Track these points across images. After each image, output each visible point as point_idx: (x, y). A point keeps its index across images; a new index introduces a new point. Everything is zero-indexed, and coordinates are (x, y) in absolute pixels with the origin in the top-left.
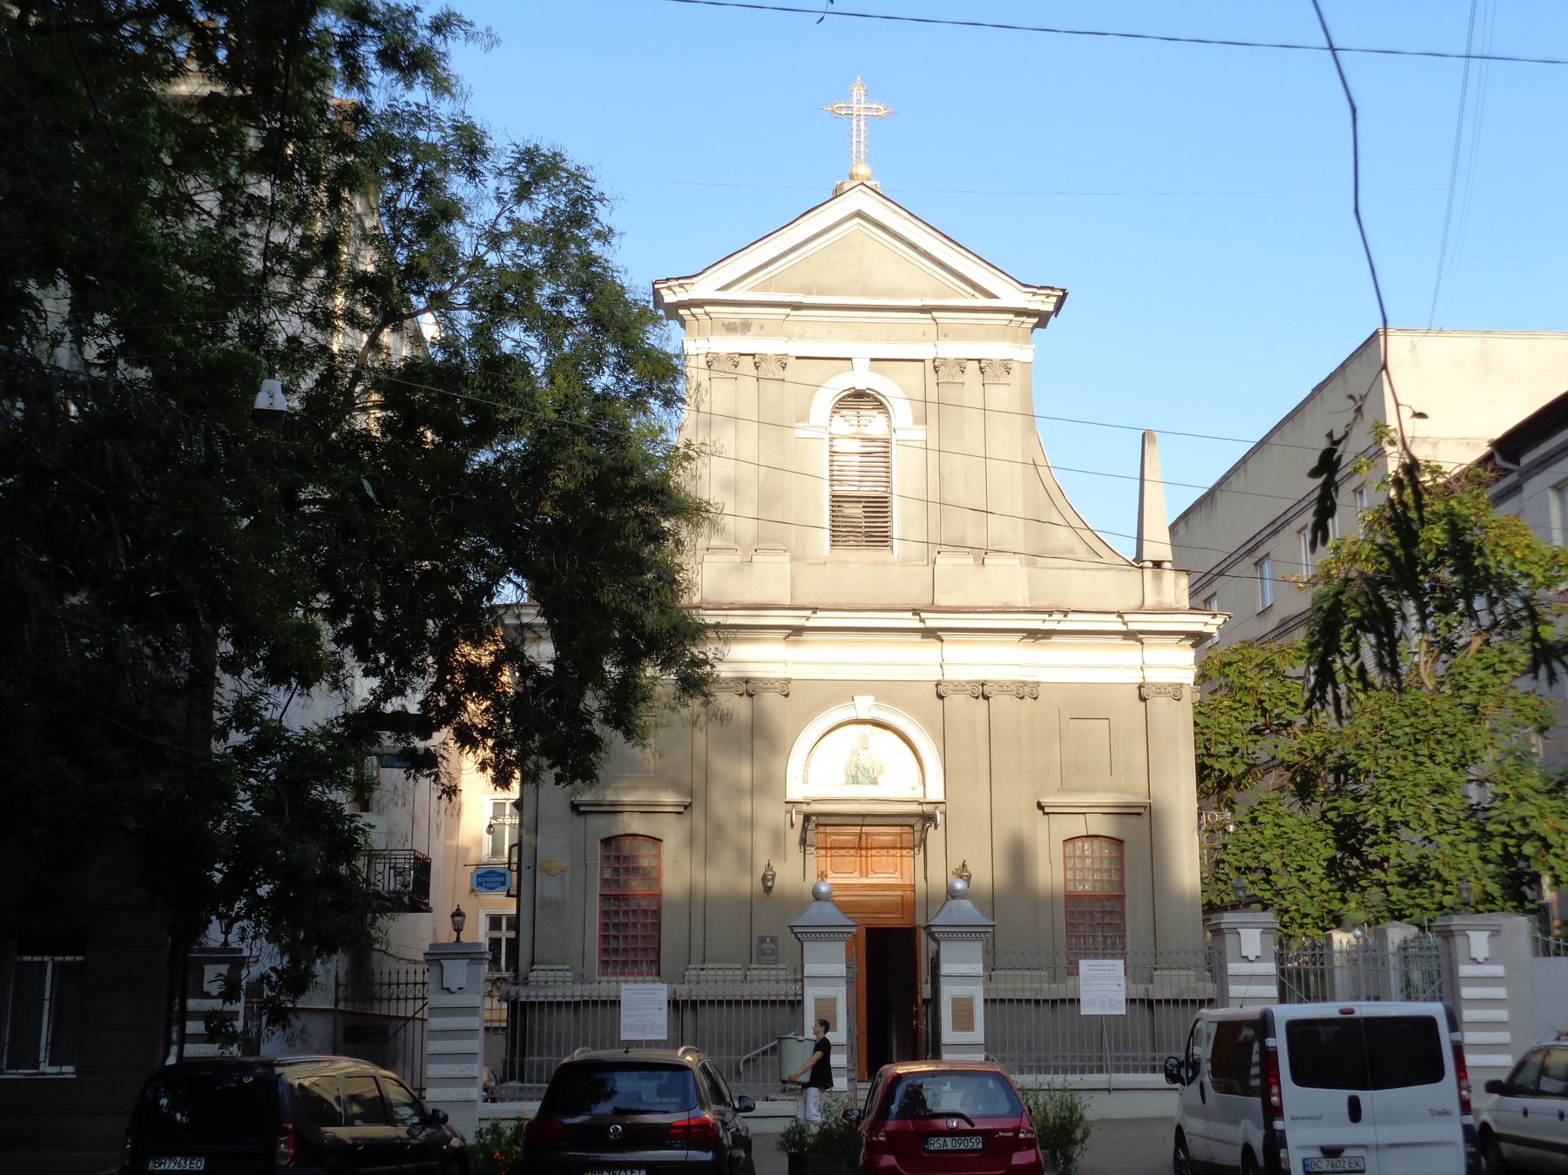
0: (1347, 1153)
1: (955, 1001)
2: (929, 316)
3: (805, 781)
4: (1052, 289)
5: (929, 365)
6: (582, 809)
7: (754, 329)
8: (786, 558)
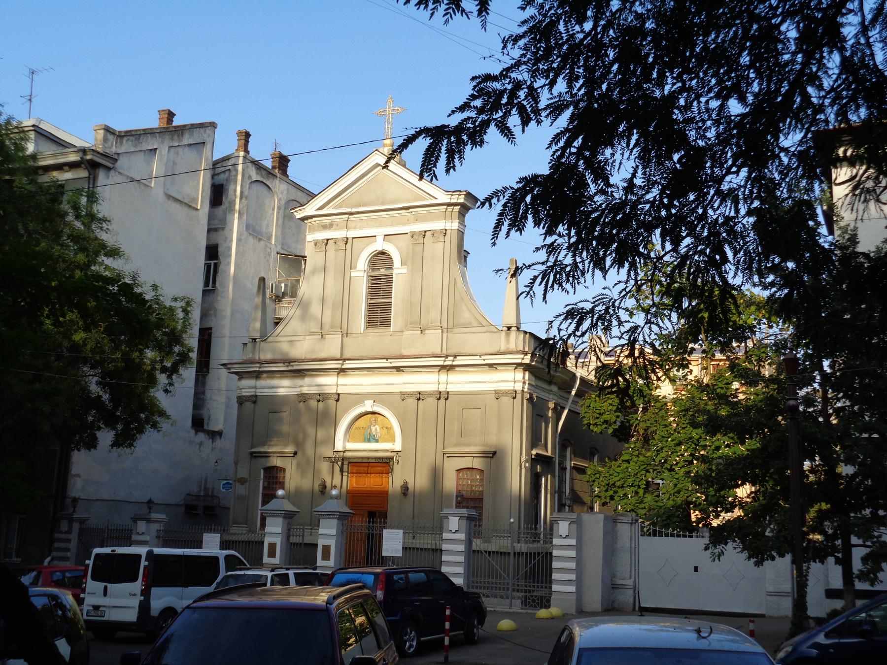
0: (101, 609)
1: (324, 546)
4: (460, 191)
7: (334, 226)
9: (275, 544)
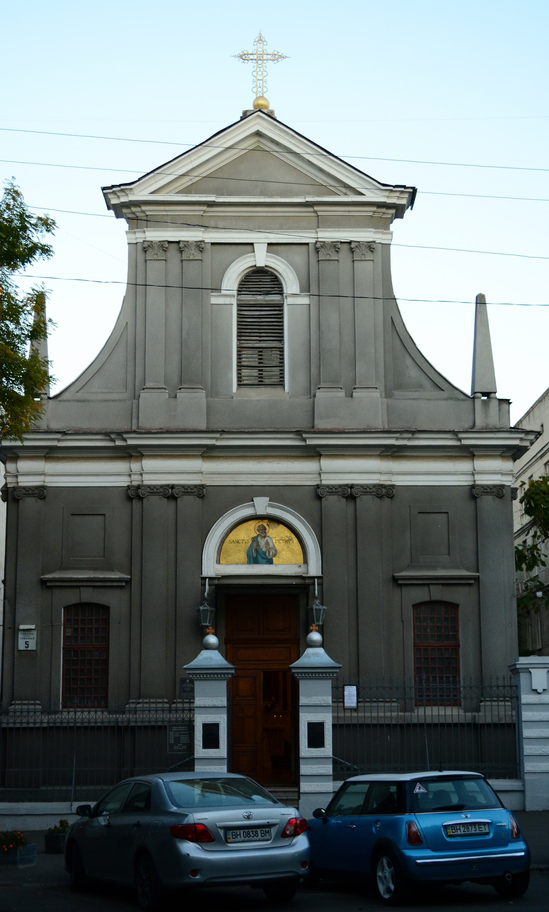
2: (311, 209)
3: (218, 562)
4: (404, 187)
5: (311, 247)
6: (48, 584)
8: (203, 394)
9: (216, 726)
